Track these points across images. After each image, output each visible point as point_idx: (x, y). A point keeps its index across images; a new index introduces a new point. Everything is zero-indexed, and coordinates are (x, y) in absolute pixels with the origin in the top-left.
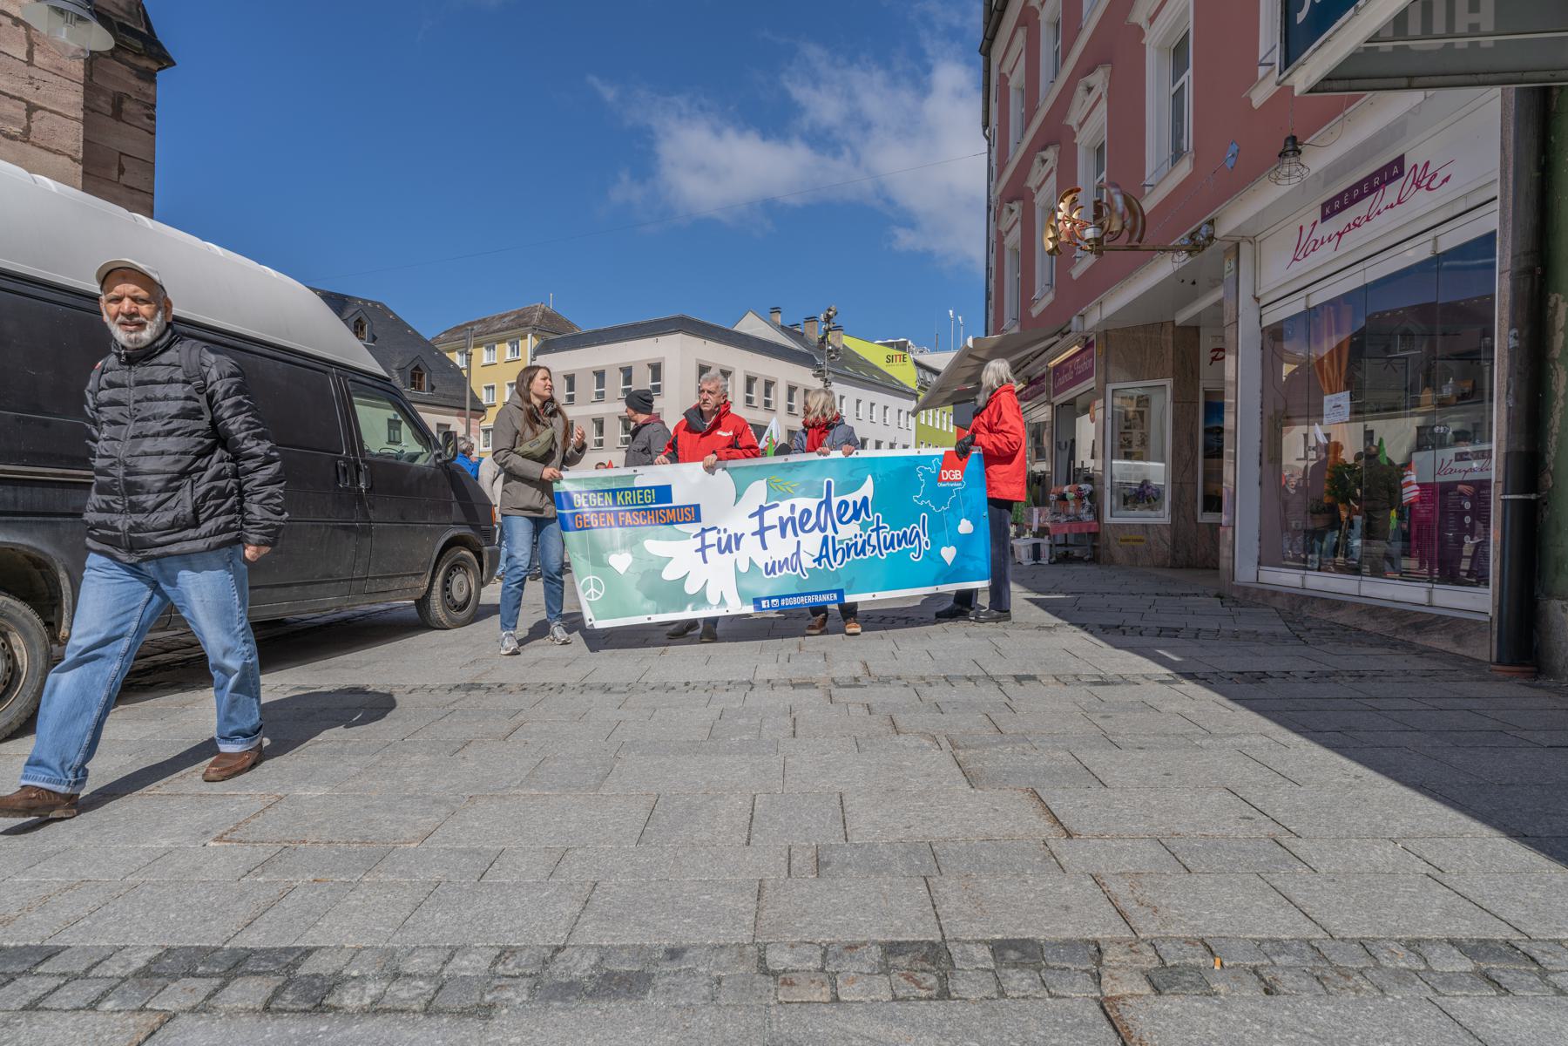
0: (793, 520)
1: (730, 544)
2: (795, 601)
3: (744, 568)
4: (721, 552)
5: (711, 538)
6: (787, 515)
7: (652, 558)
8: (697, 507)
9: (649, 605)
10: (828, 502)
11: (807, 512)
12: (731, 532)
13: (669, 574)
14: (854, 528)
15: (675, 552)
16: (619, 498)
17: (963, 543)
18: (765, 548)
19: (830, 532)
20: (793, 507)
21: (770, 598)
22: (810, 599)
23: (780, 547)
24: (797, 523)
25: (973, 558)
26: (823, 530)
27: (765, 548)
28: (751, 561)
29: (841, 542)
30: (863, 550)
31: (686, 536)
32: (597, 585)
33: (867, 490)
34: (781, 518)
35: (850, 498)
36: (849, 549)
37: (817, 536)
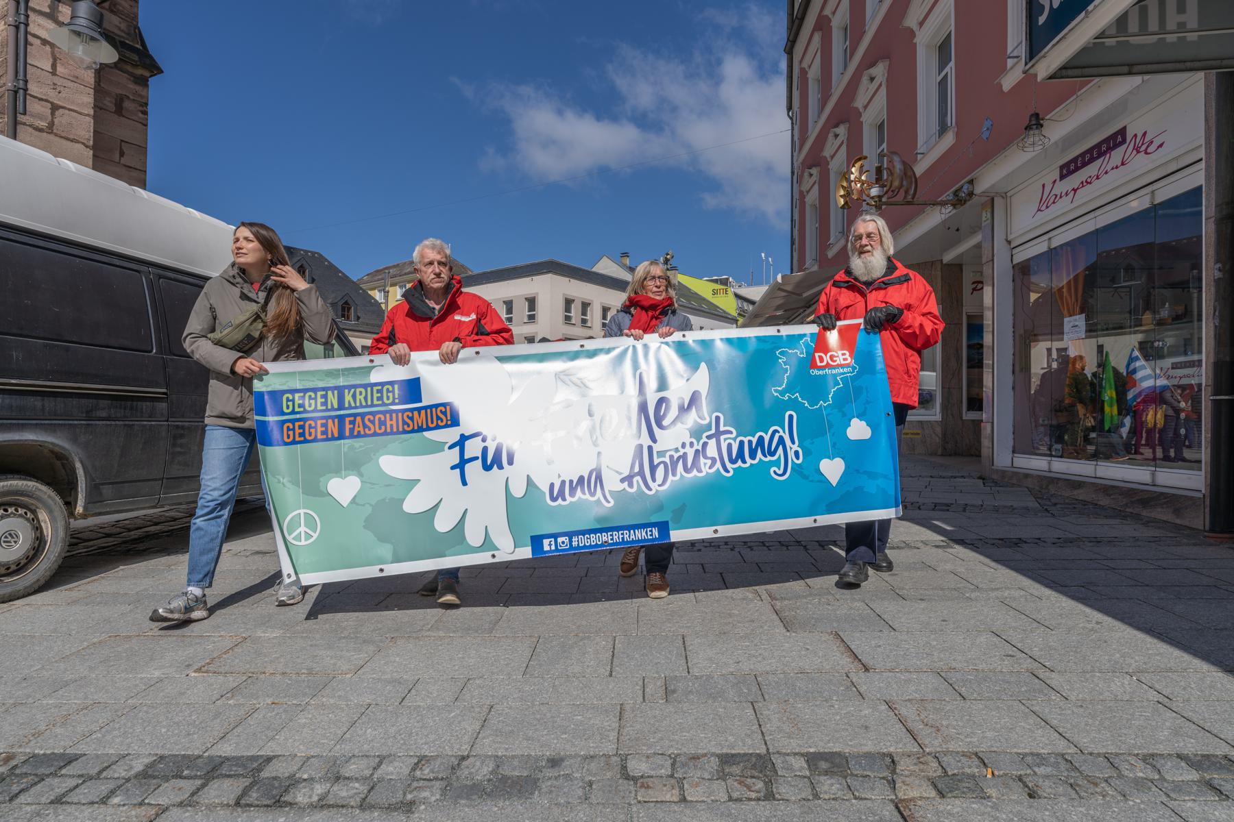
2: (594, 539)
3: (518, 490)
4: (487, 468)
5: (473, 448)
7: (392, 482)
9: (386, 550)
13: (414, 504)
15: (418, 475)
16: (348, 398)
17: (854, 453)
22: (617, 537)
25: (872, 475)
28: (529, 481)
31: (437, 447)
36: (674, 464)
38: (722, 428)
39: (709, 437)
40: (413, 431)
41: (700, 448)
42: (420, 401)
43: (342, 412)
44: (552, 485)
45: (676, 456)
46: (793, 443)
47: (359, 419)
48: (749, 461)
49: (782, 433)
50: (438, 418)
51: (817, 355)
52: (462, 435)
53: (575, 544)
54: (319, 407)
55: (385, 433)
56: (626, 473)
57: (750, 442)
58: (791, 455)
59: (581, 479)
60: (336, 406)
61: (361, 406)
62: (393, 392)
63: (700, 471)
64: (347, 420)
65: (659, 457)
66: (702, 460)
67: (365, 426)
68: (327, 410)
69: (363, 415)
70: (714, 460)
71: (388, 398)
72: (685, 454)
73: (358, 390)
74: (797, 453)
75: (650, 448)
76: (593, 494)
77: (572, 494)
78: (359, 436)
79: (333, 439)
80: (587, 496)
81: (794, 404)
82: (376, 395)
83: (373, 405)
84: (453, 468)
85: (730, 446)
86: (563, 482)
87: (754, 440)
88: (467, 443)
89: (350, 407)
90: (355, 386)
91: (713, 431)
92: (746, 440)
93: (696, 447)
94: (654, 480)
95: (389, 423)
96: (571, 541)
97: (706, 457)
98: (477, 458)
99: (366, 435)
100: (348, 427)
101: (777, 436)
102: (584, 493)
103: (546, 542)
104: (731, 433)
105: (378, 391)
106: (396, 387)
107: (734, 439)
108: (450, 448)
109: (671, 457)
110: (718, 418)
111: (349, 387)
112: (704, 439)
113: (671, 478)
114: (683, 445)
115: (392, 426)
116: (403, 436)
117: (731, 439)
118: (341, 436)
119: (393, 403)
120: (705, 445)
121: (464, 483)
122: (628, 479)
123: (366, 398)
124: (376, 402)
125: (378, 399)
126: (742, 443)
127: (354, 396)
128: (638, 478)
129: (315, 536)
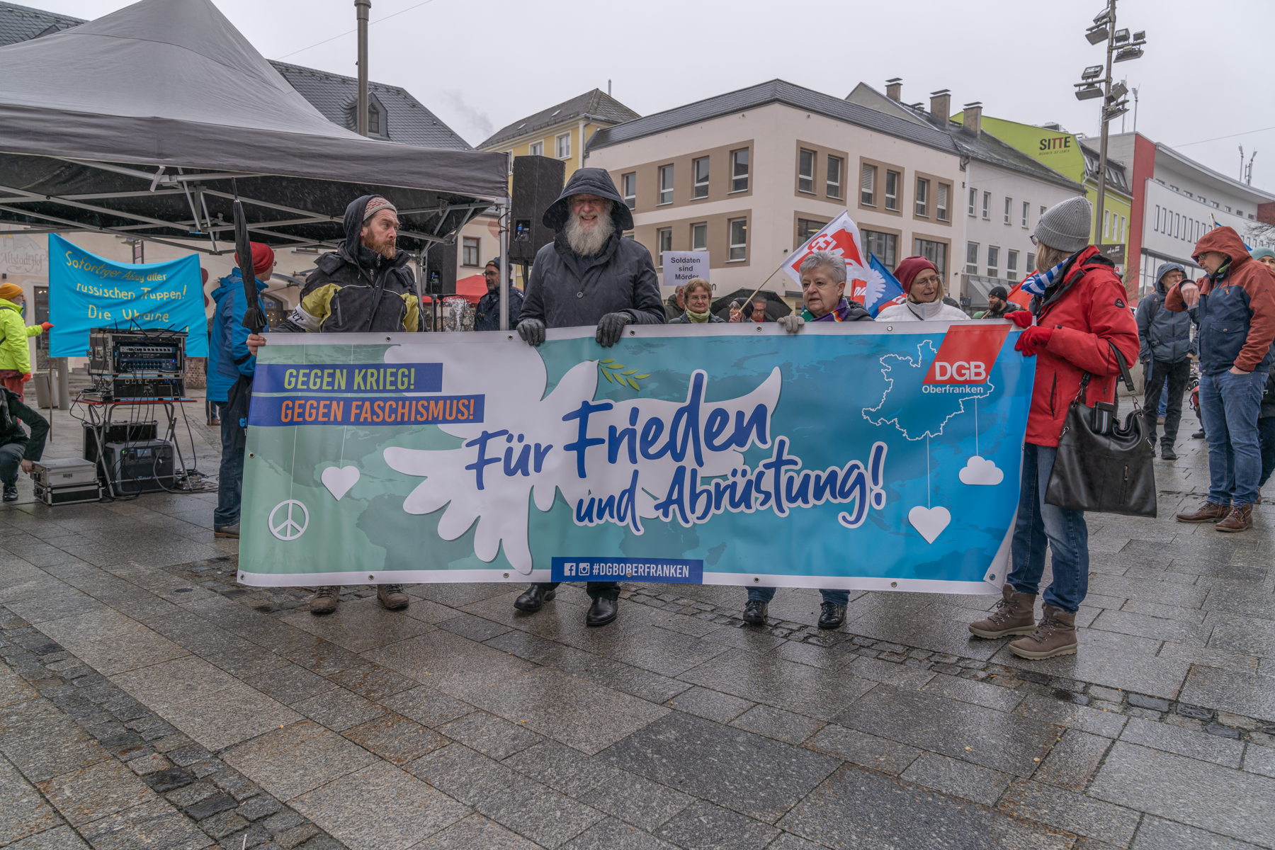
0: (631, 433)
6: (622, 424)
7: (392, 476)
8: (479, 400)
10: (692, 411)
11: (656, 423)
14: (733, 459)
15: (432, 472)
19: (689, 462)
20: (635, 413)
21: (577, 560)
24: (640, 441)
26: (678, 457)
28: (558, 493)
29: (707, 480)
30: (746, 499)
32: (299, 518)
34: (612, 429)
35: (731, 406)
36: (720, 494)
37: (668, 465)
38: (785, 457)
39: (767, 466)
40: (426, 422)
41: (753, 478)
43: (349, 395)
44: (581, 502)
46: (876, 482)
47: (367, 404)
48: (812, 501)
49: (862, 470)
50: (459, 411)
51: (938, 364)
53: (595, 572)
54: (325, 387)
55: (395, 423)
56: (663, 499)
57: (818, 478)
58: (870, 498)
59: (612, 498)
60: (343, 387)
61: (372, 391)
62: (409, 376)
64: (354, 404)
66: (754, 494)
67: (373, 413)
68: (333, 391)
69: (373, 400)
71: (403, 384)
72: (735, 484)
73: (370, 371)
74: (878, 498)
75: (694, 472)
76: (622, 519)
78: (365, 423)
79: (336, 422)
80: (616, 520)
81: (888, 434)
82: (389, 379)
83: (385, 390)
85: (791, 480)
86: (593, 500)
89: (359, 390)
90: (367, 367)
91: (773, 459)
92: (813, 474)
93: (749, 477)
94: (693, 511)
95: (400, 411)
97: (759, 490)
99: (373, 423)
100: (354, 411)
101: (856, 472)
102: (612, 516)
103: (567, 566)
104: (795, 463)
106: (413, 370)
107: (798, 472)
109: (718, 485)
110: (782, 443)
112: (761, 468)
113: (713, 510)
114: (734, 473)
115: (403, 414)
116: (414, 427)
118: (346, 421)
119: (408, 390)
120: (761, 475)
122: (664, 507)
123: (377, 381)
124: (388, 387)
125: (392, 383)
126: (807, 477)
127: (365, 378)
128: (675, 507)
129: (302, 531)
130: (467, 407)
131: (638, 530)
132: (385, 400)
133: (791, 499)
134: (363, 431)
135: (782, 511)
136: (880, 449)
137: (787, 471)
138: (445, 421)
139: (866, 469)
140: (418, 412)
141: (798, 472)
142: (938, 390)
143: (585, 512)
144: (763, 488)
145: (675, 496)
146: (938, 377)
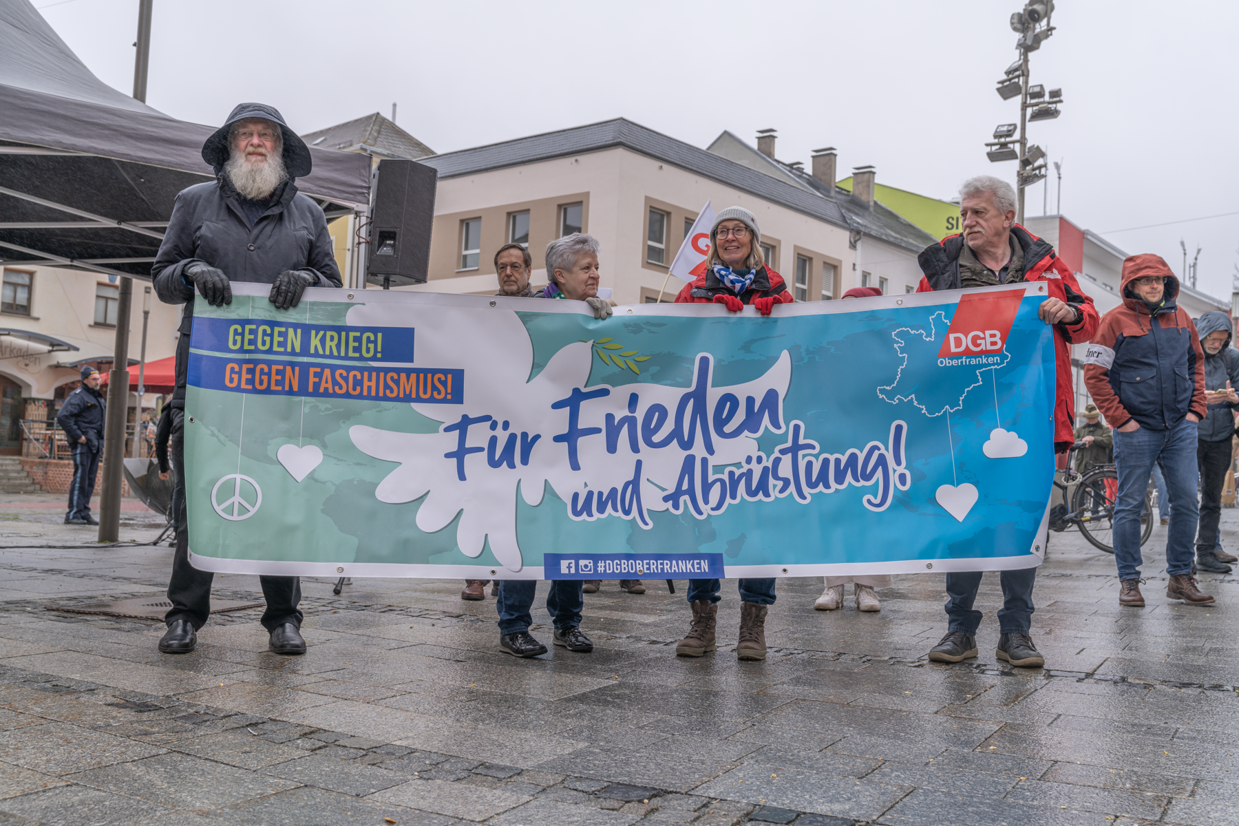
1: (514, 449)
3: (533, 496)
4: (494, 464)
5: (478, 436)
8: (458, 375)
12: (515, 429)
18: (575, 466)
23: (603, 468)
27: (575, 466)
30: (763, 487)
31: (429, 426)
33: (778, 377)
36: (734, 482)
38: (802, 441)
39: (783, 452)
40: (397, 399)
41: (770, 464)
42: (412, 361)
45: (738, 472)
50: (434, 388)
52: (465, 417)
55: (360, 397)
56: (671, 489)
57: (838, 461)
62: (375, 342)
63: (767, 495)
65: (715, 472)
66: (772, 481)
67: (335, 383)
69: (333, 368)
70: (786, 482)
71: (368, 351)
72: (750, 472)
77: (601, 509)
82: (352, 344)
83: (347, 358)
84: (448, 455)
85: (809, 464)
87: (844, 459)
88: (471, 428)
91: (789, 444)
92: (832, 458)
93: (764, 463)
94: (706, 502)
95: (366, 384)
96: (596, 566)
97: (776, 477)
98: (482, 449)
99: (335, 395)
104: (813, 447)
105: (356, 339)
106: (380, 335)
107: (817, 456)
108: (447, 430)
109: (731, 474)
110: (797, 428)
111: (318, 328)
112: (776, 454)
113: (728, 500)
114: (749, 460)
115: (369, 388)
116: (383, 403)
117: (812, 457)
119: (374, 359)
120: (777, 461)
121: (462, 477)
122: (673, 498)
124: (351, 354)
125: (356, 350)
126: (826, 461)
128: (686, 497)
130: (444, 383)
131: (646, 524)
132: (349, 369)
133: (812, 485)
134: (324, 404)
135: (804, 498)
136: (899, 428)
137: (804, 456)
138: (419, 400)
139: (887, 449)
140: (387, 386)
141: (817, 456)
142: (954, 362)
143: (584, 504)
144: (781, 474)
145: (685, 486)
146: (953, 349)
